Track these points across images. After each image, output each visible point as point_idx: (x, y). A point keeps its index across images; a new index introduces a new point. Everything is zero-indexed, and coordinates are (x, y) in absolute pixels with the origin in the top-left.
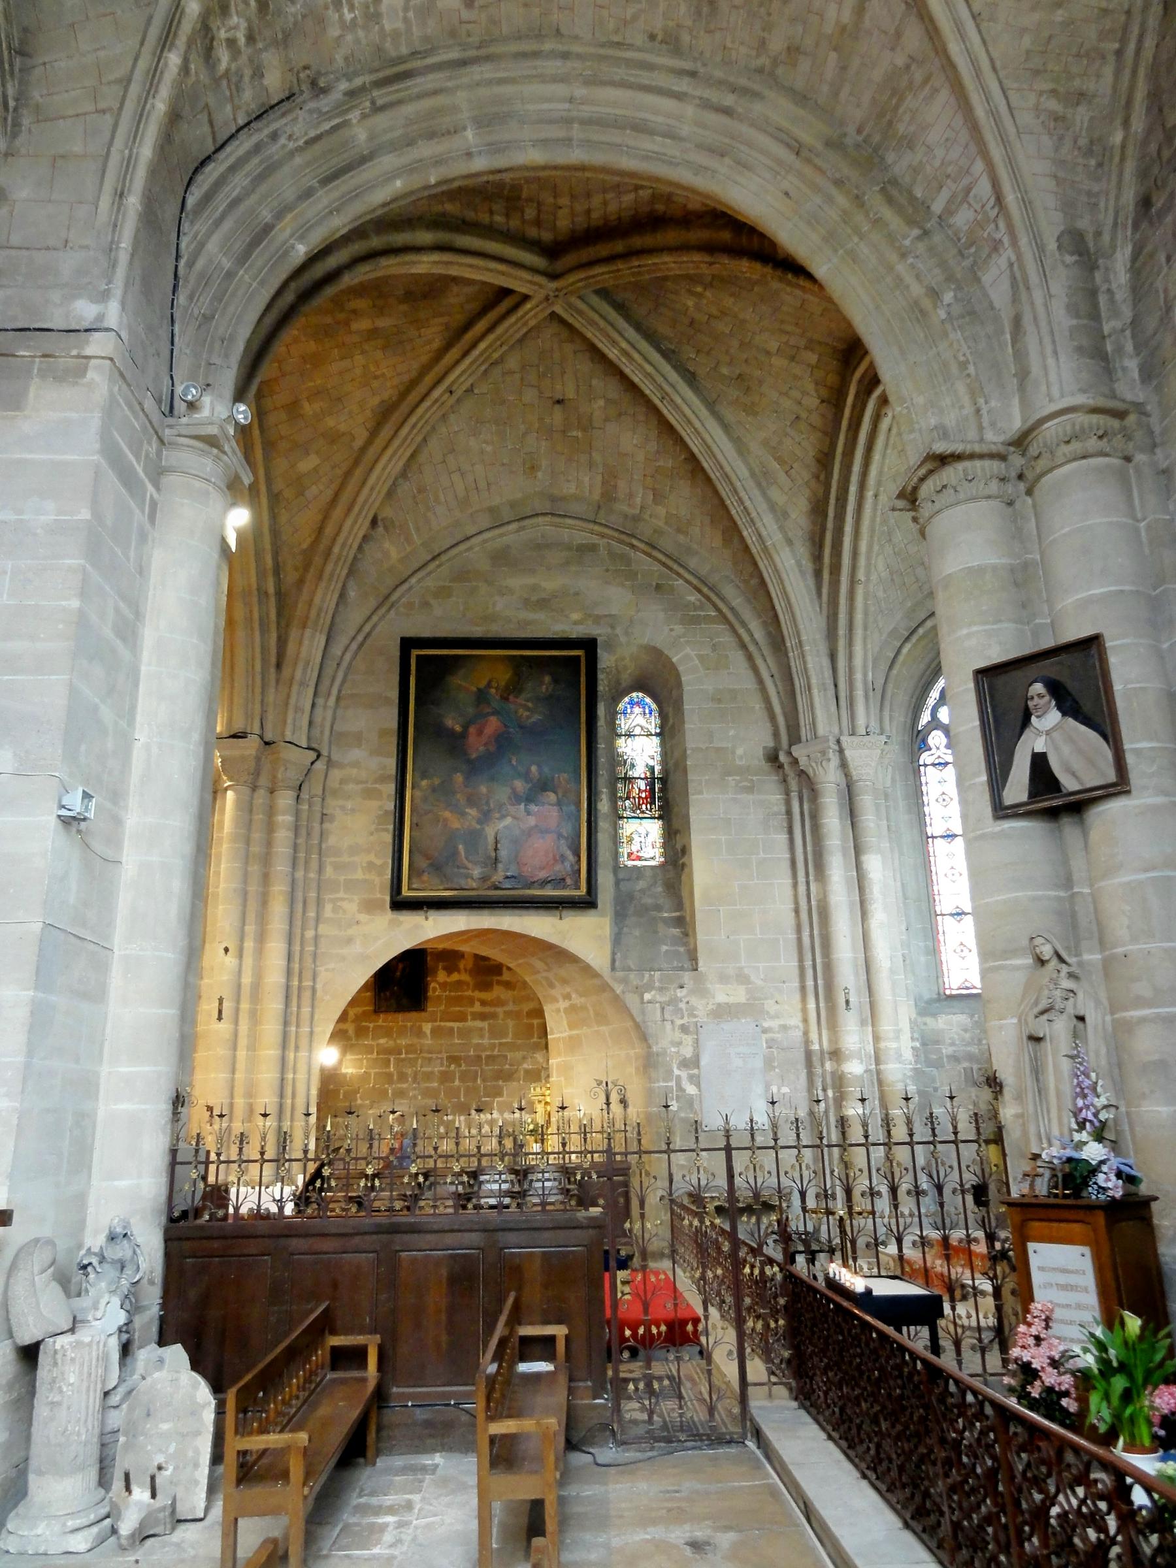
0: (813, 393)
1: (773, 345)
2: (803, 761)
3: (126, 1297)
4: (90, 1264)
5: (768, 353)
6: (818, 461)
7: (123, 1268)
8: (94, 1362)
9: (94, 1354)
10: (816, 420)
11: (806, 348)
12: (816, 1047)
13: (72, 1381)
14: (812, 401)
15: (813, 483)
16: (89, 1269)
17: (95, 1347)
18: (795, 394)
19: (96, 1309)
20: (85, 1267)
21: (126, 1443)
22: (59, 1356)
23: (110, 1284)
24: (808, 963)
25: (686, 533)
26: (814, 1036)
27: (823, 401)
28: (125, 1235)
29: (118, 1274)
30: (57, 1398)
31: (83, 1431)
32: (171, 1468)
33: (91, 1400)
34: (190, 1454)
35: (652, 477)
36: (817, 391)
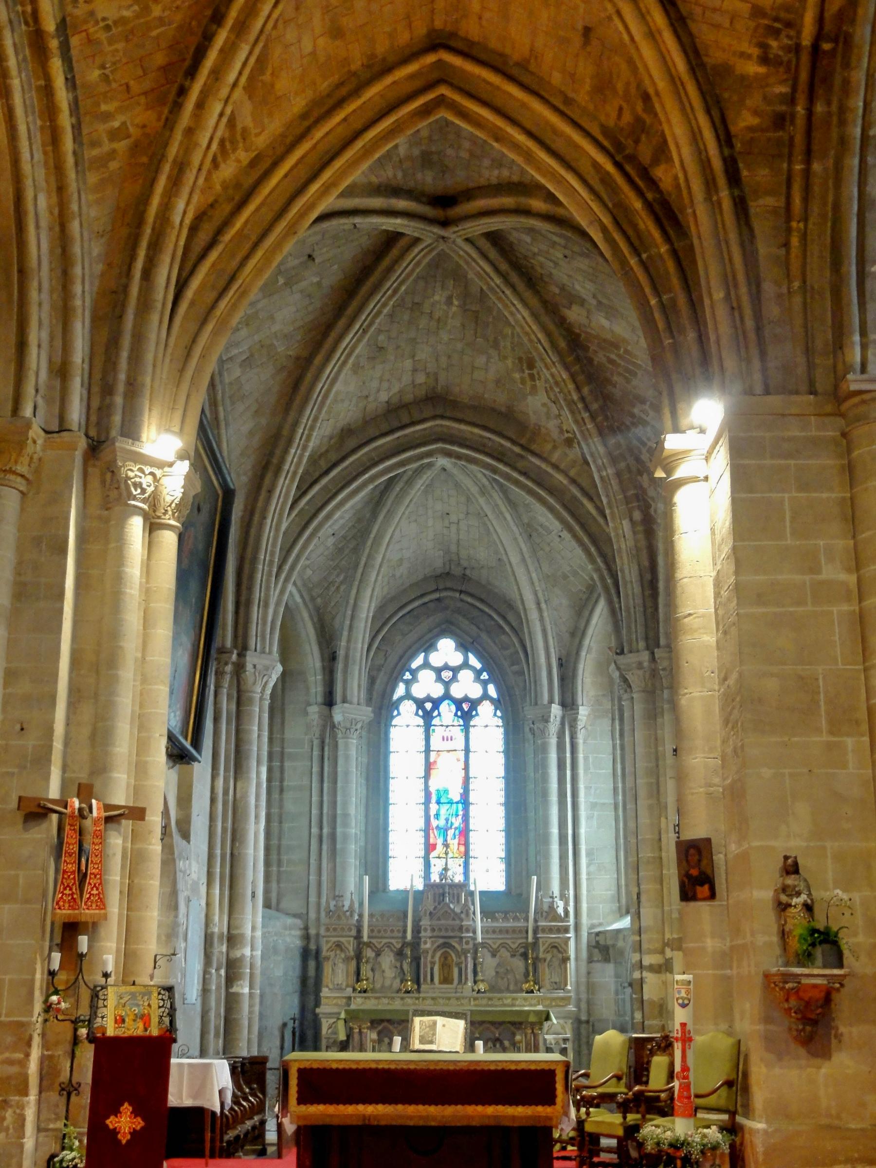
0: (391, 394)
1: (421, 355)
2: (249, 667)
5: (413, 357)
6: (342, 430)
10: (372, 407)
11: (428, 375)
12: (216, 930)
14: (384, 397)
15: (326, 440)
18: (385, 385)
24: (218, 852)
25: (233, 403)
26: (216, 918)
27: (387, 402)
35: (262, 346)
36: (395, 394)
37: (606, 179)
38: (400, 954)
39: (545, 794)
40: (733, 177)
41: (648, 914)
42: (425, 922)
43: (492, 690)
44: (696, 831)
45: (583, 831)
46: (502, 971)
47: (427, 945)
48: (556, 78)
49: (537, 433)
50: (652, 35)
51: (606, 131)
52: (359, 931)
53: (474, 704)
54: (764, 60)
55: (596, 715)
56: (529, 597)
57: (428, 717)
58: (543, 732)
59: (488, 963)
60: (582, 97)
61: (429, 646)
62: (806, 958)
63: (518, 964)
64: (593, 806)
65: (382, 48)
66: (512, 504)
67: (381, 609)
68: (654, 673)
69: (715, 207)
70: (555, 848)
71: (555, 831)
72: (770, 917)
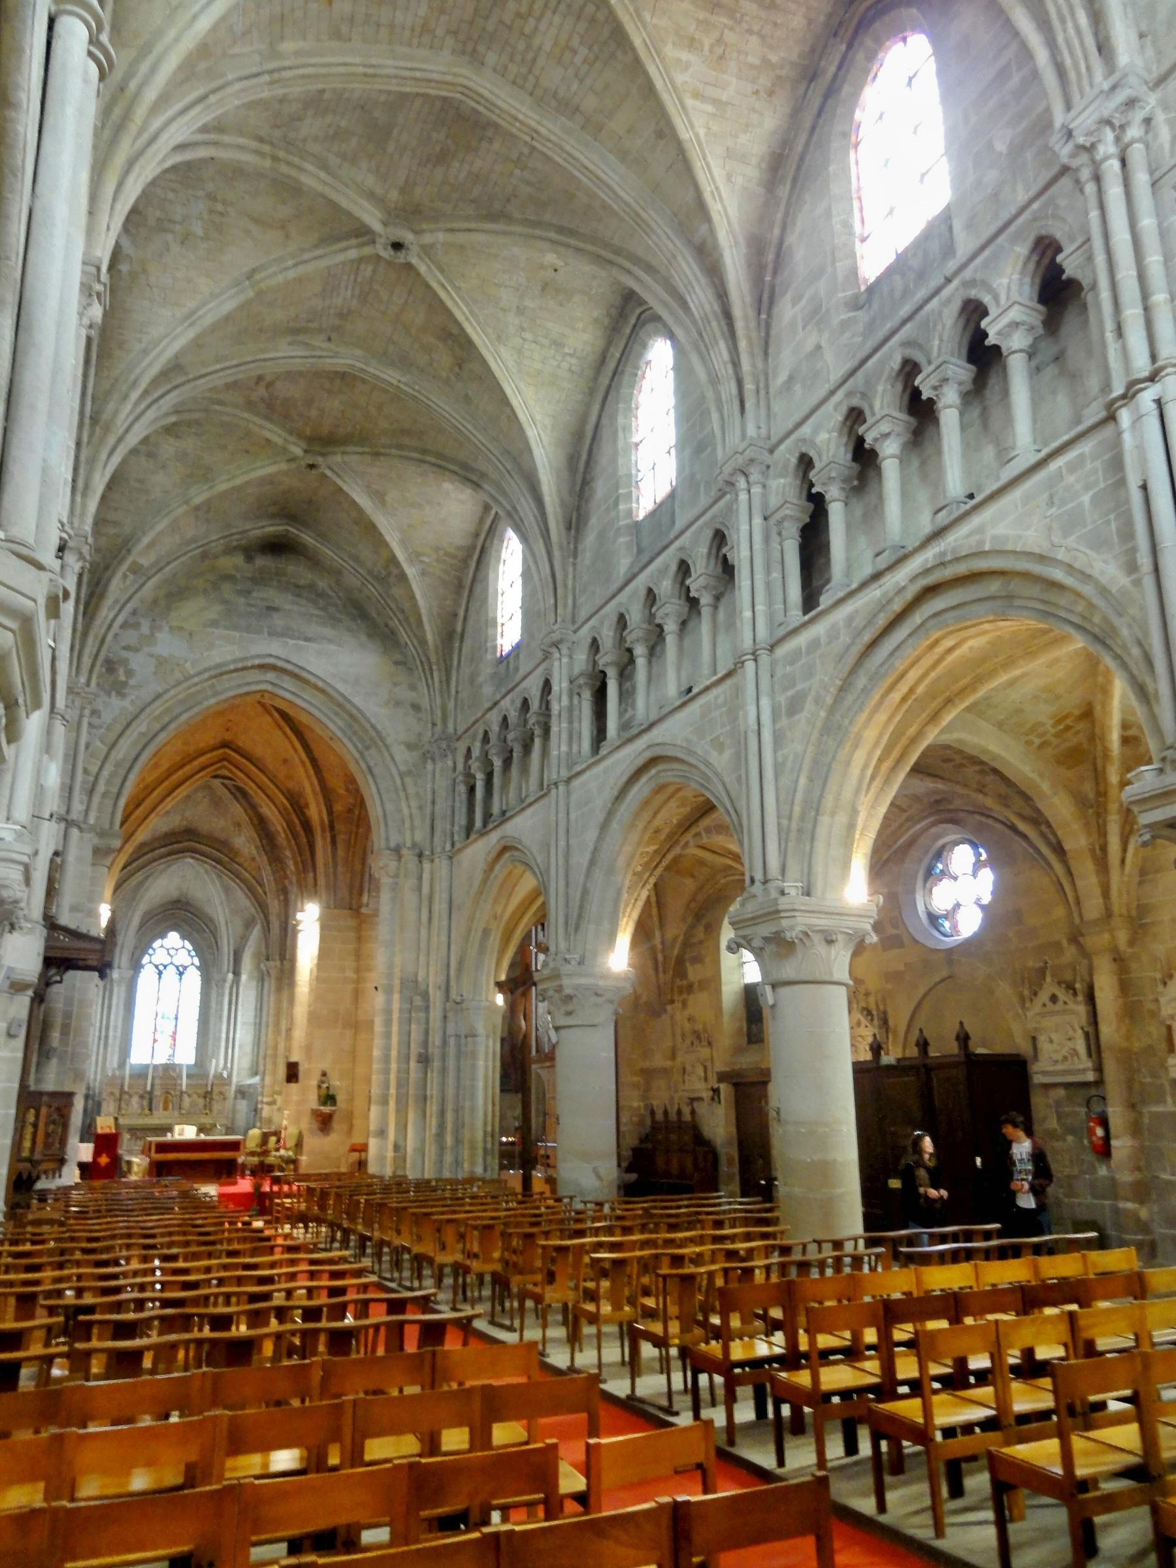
37: (285, 809)
38: (142, 1097)
39: (221, 1017)
40: (332, 828)
41: (268, 1079)
42: (157, 1082)
43: (196, 961)
44: (293, 1059)
45: (238, 1035)
46: (193, 1104)
47: (157, 1092)
48: (271, 767)
49: (237, 853)
50: (308, 777)
51: (289, 791)
52: (122, 1086)
53: (185, 968)
54: (347, 790)
55: (250, 978)
56: (222, 919)
57: (160, 973)
58: (223, 987)
59: (187, 1101)
60: (281, 776)
61: (163, 935)
62: (324, 1104)
63: (201, 1101)
64: (244, 1023)
65: (202, 745)
66: (219, 876)
67: (143, 917)
68: (282, 971)
69: (324, 839)
70: (223, 1044)
71: (224, 1036)
72: (315, 1090)
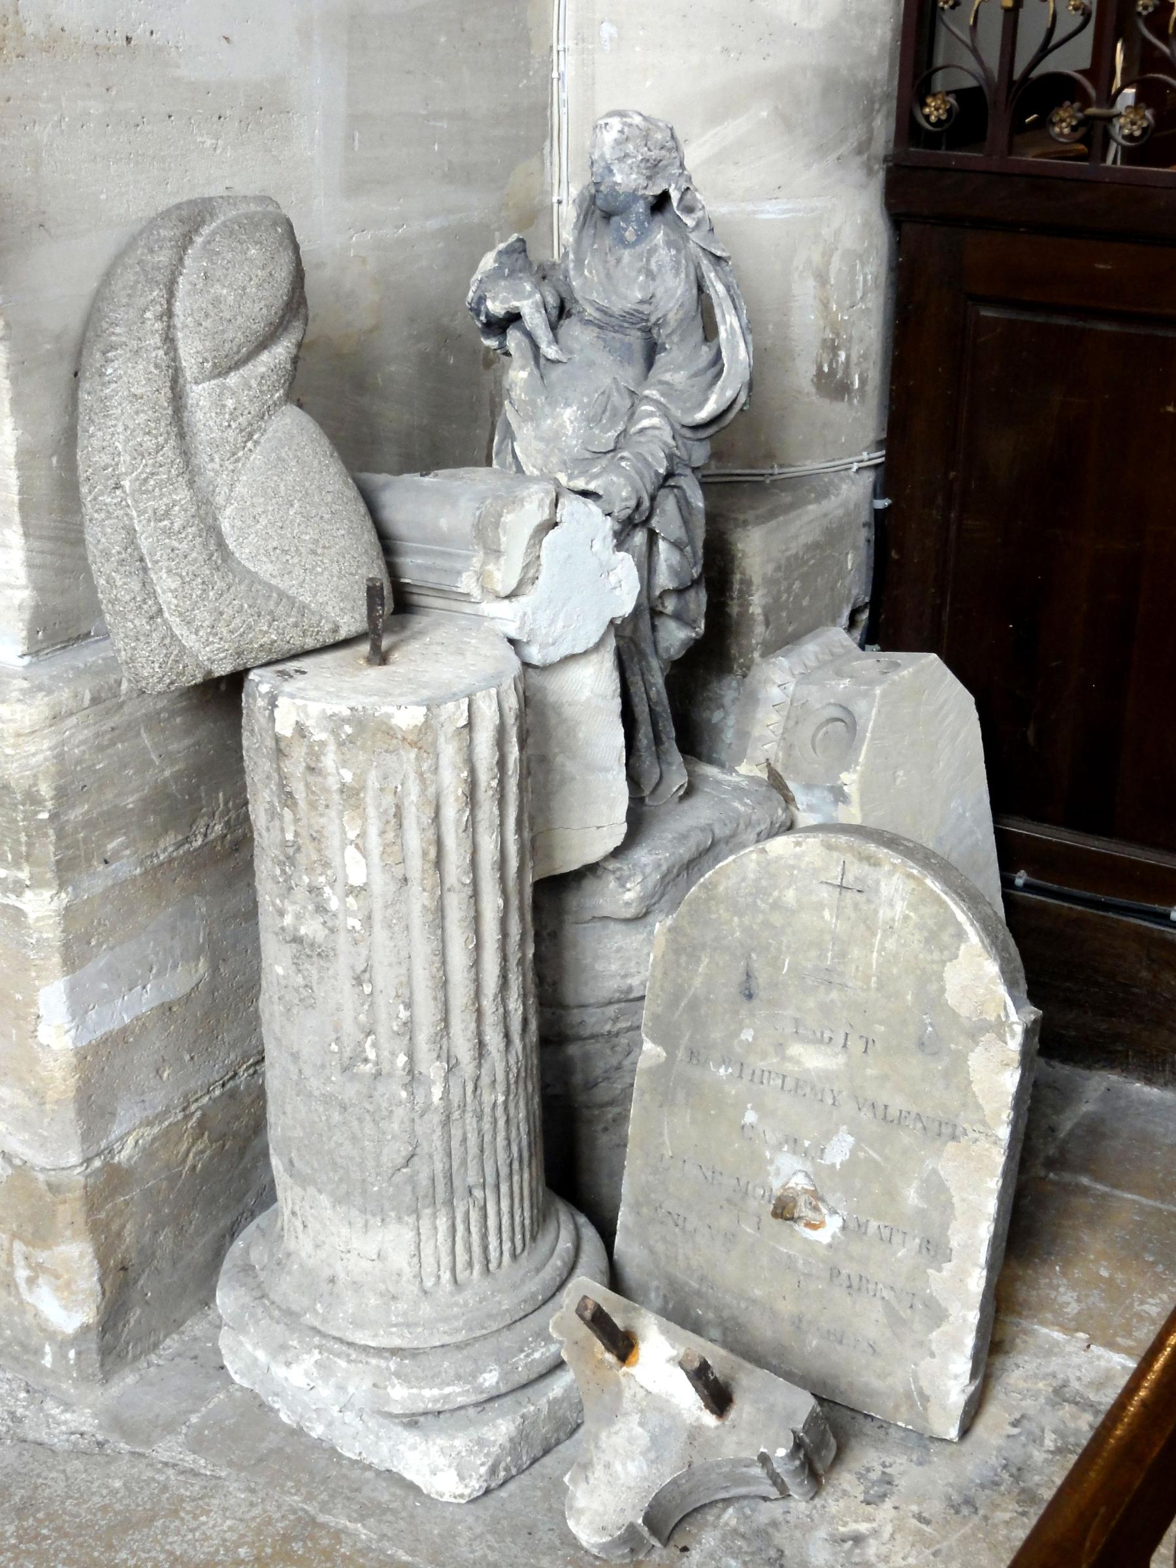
3: (666, 480)
4: (514, 318)
7: (652, 351)
8: (452, 812)
9: (451, 782)
13: (357, 877)
16: (514, 339)
17: (449, 752)
19: (494, 552)
20: (501, 325)
21: (661, 1072)
22: (295, 767)
23: (592, 420)
28: (661, 203)
29: (629, 375)
30: (312, 928)
31: (433, 1070)
32: (833, 1224)
33: (459, 958)
34: (912, 1196)
